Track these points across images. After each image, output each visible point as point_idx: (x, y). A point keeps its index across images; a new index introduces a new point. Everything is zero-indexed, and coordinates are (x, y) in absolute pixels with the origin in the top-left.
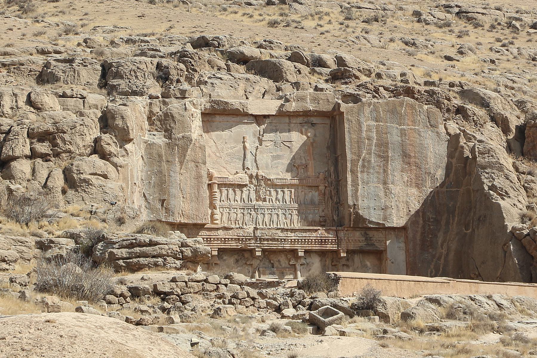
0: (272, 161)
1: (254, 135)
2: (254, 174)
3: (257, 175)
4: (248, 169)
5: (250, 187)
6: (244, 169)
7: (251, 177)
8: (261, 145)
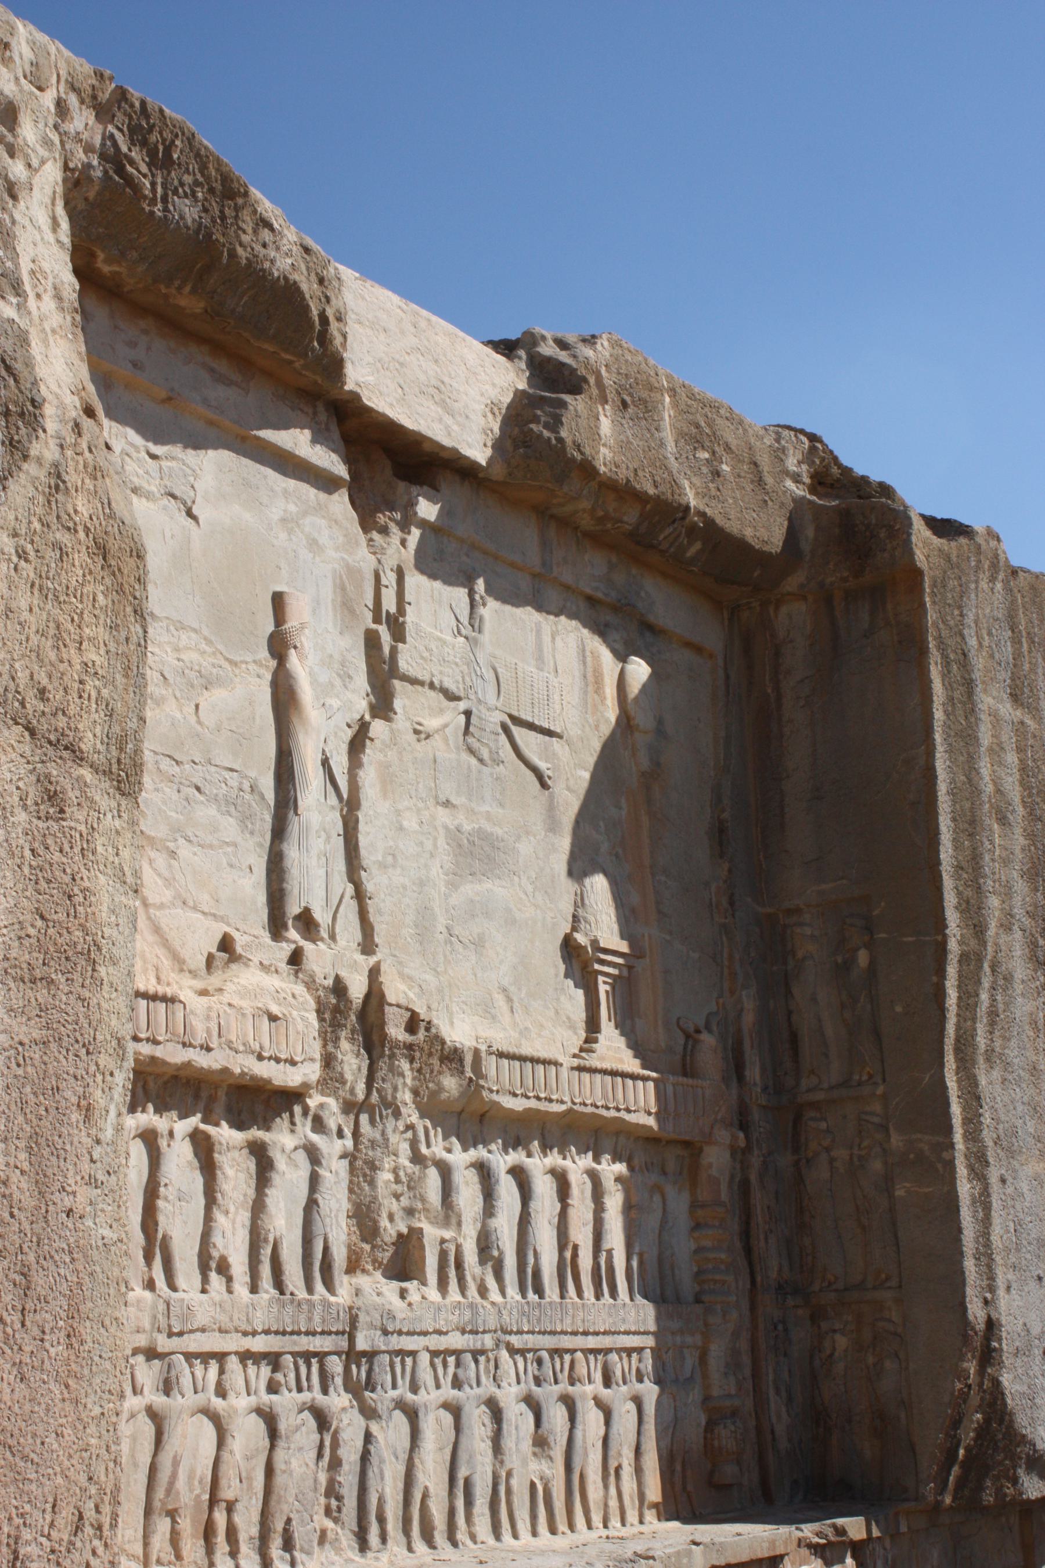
0: (456, 878)
1: (346, 607)
2: (357, 989)
3: (375, 996)
4: (307, 922)
5: (319, 1125)
6: (276, 926)
8: (382, 705)
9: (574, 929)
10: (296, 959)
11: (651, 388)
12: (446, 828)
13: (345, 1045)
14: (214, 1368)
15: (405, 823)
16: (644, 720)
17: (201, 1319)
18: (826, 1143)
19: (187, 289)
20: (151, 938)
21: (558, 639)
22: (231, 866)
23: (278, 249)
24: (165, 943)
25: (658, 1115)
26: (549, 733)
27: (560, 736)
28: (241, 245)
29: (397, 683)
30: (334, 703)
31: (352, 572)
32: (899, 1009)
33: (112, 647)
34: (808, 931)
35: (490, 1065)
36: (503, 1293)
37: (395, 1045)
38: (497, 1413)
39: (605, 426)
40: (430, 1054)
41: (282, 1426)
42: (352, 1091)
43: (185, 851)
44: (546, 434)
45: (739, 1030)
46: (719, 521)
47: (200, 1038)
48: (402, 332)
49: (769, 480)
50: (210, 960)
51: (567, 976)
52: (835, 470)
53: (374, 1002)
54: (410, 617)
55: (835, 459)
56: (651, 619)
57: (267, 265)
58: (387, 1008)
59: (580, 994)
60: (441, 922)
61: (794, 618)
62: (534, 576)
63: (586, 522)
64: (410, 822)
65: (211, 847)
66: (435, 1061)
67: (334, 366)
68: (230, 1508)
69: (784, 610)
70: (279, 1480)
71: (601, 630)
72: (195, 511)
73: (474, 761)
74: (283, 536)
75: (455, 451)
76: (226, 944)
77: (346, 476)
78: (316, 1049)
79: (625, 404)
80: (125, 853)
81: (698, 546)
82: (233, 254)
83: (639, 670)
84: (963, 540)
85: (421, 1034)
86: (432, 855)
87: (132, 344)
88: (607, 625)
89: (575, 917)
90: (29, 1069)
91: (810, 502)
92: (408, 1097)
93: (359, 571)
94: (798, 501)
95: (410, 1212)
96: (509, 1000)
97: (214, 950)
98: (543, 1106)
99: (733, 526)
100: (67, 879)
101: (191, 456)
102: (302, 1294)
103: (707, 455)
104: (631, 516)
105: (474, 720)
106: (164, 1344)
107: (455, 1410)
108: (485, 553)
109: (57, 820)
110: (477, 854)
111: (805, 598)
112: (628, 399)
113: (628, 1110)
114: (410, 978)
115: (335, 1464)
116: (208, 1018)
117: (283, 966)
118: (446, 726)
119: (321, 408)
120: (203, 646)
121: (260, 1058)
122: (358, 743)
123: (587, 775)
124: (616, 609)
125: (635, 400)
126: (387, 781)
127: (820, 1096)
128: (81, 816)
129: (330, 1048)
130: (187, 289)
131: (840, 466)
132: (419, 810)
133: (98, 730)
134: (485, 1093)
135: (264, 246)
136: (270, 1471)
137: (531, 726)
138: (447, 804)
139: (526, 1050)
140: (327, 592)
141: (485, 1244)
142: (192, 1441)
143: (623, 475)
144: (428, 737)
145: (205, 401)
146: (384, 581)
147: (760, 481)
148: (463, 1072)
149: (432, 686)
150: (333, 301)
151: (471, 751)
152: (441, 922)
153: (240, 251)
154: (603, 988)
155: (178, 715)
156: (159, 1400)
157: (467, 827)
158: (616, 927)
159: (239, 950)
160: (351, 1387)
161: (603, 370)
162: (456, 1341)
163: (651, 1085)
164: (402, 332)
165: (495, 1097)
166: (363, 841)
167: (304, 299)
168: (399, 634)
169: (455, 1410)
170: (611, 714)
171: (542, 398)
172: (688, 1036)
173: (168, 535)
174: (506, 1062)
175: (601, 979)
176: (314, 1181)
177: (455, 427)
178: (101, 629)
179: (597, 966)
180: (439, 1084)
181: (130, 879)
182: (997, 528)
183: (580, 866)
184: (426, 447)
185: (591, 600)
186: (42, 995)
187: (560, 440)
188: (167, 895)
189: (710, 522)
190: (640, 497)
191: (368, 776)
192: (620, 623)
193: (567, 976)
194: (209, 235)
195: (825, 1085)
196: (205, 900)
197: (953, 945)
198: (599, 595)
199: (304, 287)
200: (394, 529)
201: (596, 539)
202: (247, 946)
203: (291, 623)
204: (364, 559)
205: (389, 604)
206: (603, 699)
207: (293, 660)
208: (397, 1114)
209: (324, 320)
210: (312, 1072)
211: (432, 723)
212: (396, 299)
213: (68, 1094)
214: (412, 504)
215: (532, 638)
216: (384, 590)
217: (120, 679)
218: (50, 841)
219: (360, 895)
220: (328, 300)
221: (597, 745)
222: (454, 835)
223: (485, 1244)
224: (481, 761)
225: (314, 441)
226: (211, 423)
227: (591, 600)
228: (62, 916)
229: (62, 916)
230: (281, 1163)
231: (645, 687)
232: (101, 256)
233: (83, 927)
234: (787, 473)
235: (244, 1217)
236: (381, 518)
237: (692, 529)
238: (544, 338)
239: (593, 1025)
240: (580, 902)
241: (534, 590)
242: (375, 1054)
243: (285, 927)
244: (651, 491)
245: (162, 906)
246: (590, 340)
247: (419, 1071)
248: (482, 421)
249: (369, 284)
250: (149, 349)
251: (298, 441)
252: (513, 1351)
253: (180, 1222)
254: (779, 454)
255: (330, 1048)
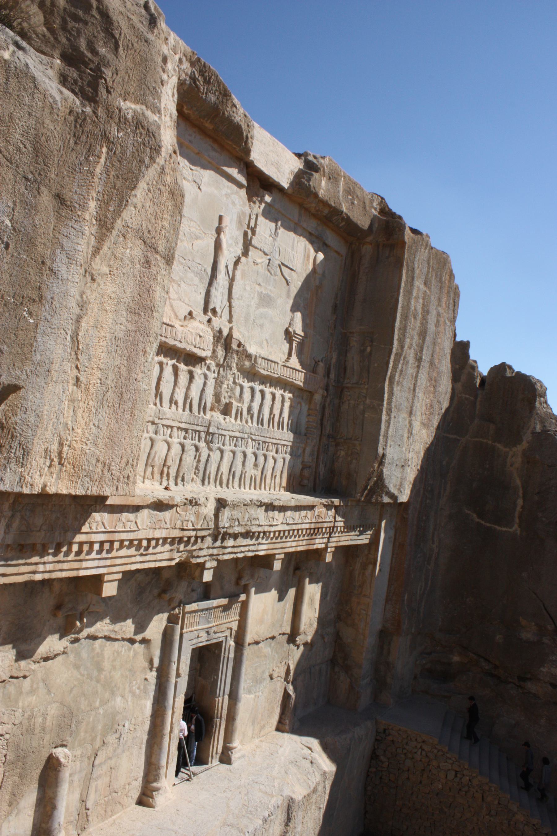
0: (258, 306)
1: (240, 222)
2: (225, 333)
3: (230, 336)
4: (214, 311)
5: (209, 368)
6: (205, 311)
7: (218, 336)
8: (245, 253)
9: (289, 326)
10: (209, 321)
11: (338, 175)
12: (258, 291)
13: (219, 348)
14: (169, 430)
15: (247, 288)
16: (319, 271)
17: (168, 416)
18: (349, 398)
19: (209, 121)
20: (169, 308)
21: (299, 244)
22: (195, 291)
23: (237, 114)
24: (173, 310)
25: (304, 383)
26: (292, 270)
27: (295, 271)
28: (227, 111)
29: (251, 247)
30: (232, 250)
31: (243, 213)
32: (376, 365)
33: (171, 222)
34: (355, 339)
35: (259, 360)
36: (252, 423)
37: (233, 350)
38: (245, 456)
39: (323, 183)
40: (243, 354)
41: (186, 449)
42: (219, 361)
43: (183, 285)
44: (306, 182)
45: (331, 363)
46: (351, 217)
47: (179, 338)
48: (269, 145)
49: (368, 208)
50: (185, 317)
51: (285, 339)
52: (387, 209)
53: (229, 337)
54: (258, 229)
55: (388, 206)
56: (327, 242)
57: (233, 118)
58: (233, 340)
59: (288, 345)
60: (252, 318)
61: (367, 249)
62: (296, 224)
63: (313, 210)
64: (248, 288)
65: (190, 285)
66: (244, 357)
67: (248, 152)
68: (169, 468)
69: (365, 247)
70: (183, 463)
71: (312, 243)
72: (201, 187)
73: (269, 274)
74: (225, 199)
75: (279, 183)
76: (190, 313)
77: (246, 185)
78: (211, 347)
79: (330, 178)
80: (166, 282)
81: (344, 223)
82: (224, 113)
83: (321, 256)
84: (419, 236)
85: (241, 348)
86: (253, 298)
87: (190, 135)
88: (314, 242)
89: (290, 323)
90: (130, 338)
91: (378, 217)
92: (235, 365)
93: (245, 213)
94: (375, 216)
95: (230, 397)
96: (268, 343)
97: (187, 315)
98: (272, 374)
99: (355, 219)
100: (148, 286)
101: (202, 171)
102: (197, 414)
103: (351, 197)
104: (326, 211)
105: (271, 262)
106: (157, 421)
107: (234, 453)
108: (283, 214)
109: (148, 269)
110: (266, 300)
111: (371, 244)
112: (331, 177)
113: (295, 380)
114: (241, 332)
115: (199, 461)
116: (182, 333)
117: (206, 322)
118: (262, 262)
119: (242, 164)
120: (197, 227)
121: (195, 347)
122: (237, 263)
123: (300, 284)
124: (317, 237)
125: (333, 178)
126: (243, 275)
127: (349, 385)
128: (155, 269)
129: (215, 348)
130: (209, 121)
131: (388, 208)
132: (251, 285)
133: (163, 245)
134: (256, 368)
135: (233, 112)
136: (181, 460)
137: (287, 267)
138: (259, 285)
139: (270, 358)
140: (235, 218)
141: (249, 409)
142: (161, 449)
143: (326, 199)
144: (257, 264)
145: (209, 156)
146: (252, 217)
147: (365, 208)
148: (251, 361)
149: (261, 250)
150: (251, 132)
151: (269, 271)
152: (252, 318)
153: (226, 113)
154: (295, 344)
155: (187, 246)
156: (154, 436)
157: (264, 292)
158: (301, 328)
159: (194, 316)
160: (206, 441)
161: (326, 167)
162: (237, 434)
163: (303, 374)
164: (269, 145)
165: (259, 369)
166: (234, 291)
167: (242, 130)
168: (254, 233)
169: (234, 453)
170: (310, 267)
171: (307, 172)
172: (316, 362)
173: (192, 192)
174: (264, 360)
175: (294, 342)
176: (205, 384)
177: (280, 176)
178: (169, 216)
179: (294, 338)
180: (244, 363)
181: (166, 289)
182: (429, 235)
183: (294, 309)
184: (271, 180)
185: (311, 234)
186: (137, 318)
187: (310, 185)
188: (176, 297)
189: (348, 217)
190: (330, 206)
191: (238, 273)
192: (318, 242)
193: (285, 339)
194: (218, 106)
195: (351, 383)
196: (186, 300)
197: (394, 350)
198: (313, 233)
199: (243, 127)
200: (257, 203)
201: (315, 216)
202: (196, 315)
203: (223, 225)
204: (247, 210)
205: (252, 224)
206: (309, 263)
207: (222, 236)
208: (231, 369)
209: (247, 138)
210: (209, 353)
211: (259, 261)
212: (269, 135)
213: (140, 347)
214: (264, 196)
215: (292, 241)
216: (251, 220)
217: (172, 231)
218: (145, 275)
219: (230, 306)
220: (249, 132)
221: (305, 276)
222: (260, 294)
223: (249, 409)
224: (271, 274)
225: (239, 173)
226: (209, 162)
227: (311, 234)
228: (145, 296)
229: (145, 296)
230: (196, 377)
231: (321, 261)
232: (185, 107)
233: (151, 301)
234: (373, 207)
235: (184, 390)
236: (254, 199)
237: (343, 219)
238: (310, 154)
239: (290, 354)
240: (292, 319)
241: (294, 227)
242: (228, 351)
243: (208, 311)
244: (333, 205)
245: (174, 300)
246: (323, 158)
247: (239, 358)
248: (288, 176)
249: (262, 129)
250: (195, 137)
251: (234, 172)
252: (252, 440)
253: (166, 388)
254: (372, 201)
255: (215, 348)
